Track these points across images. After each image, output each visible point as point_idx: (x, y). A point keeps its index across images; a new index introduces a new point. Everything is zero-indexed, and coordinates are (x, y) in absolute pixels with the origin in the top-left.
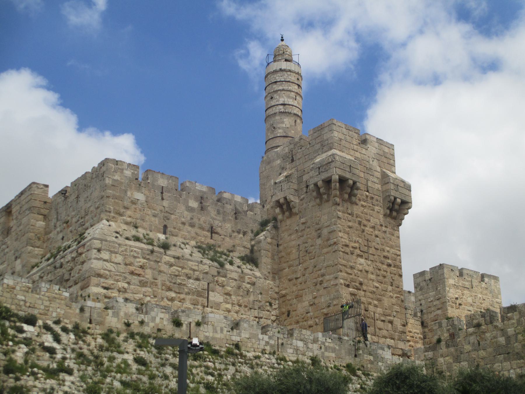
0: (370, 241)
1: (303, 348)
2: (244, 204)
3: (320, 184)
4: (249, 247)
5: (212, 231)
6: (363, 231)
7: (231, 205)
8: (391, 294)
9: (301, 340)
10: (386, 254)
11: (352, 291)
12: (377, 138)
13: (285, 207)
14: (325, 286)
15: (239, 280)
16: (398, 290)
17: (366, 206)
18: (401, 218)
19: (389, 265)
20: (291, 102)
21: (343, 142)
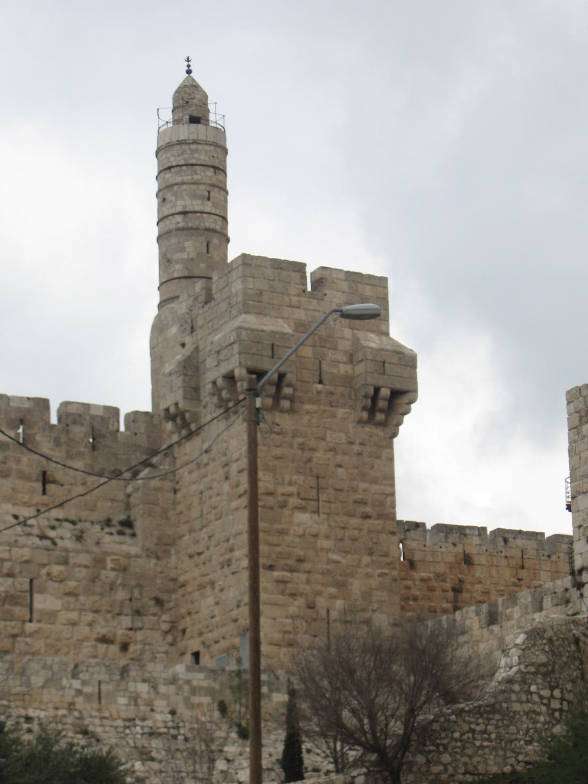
0: (324, 478)
1: (149, 693)
2: (109, 418)
3: (220, 382)
4: (122, 497)
5: (45, 479)
6: (310, 460)
7: (82, 424)
8: (370, 570)
9: (144, 681)
10: (358, 496)
11: (278, 576)
12: (348, 273)
13: (178, 420)
14: (234, 570)
15: (94, 566)
16: (387, 560)
17: (316, 412)
18: (395, 422)
19: (366, 517)
20: (197, 206)
21: (266, 297)
